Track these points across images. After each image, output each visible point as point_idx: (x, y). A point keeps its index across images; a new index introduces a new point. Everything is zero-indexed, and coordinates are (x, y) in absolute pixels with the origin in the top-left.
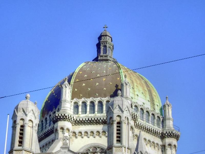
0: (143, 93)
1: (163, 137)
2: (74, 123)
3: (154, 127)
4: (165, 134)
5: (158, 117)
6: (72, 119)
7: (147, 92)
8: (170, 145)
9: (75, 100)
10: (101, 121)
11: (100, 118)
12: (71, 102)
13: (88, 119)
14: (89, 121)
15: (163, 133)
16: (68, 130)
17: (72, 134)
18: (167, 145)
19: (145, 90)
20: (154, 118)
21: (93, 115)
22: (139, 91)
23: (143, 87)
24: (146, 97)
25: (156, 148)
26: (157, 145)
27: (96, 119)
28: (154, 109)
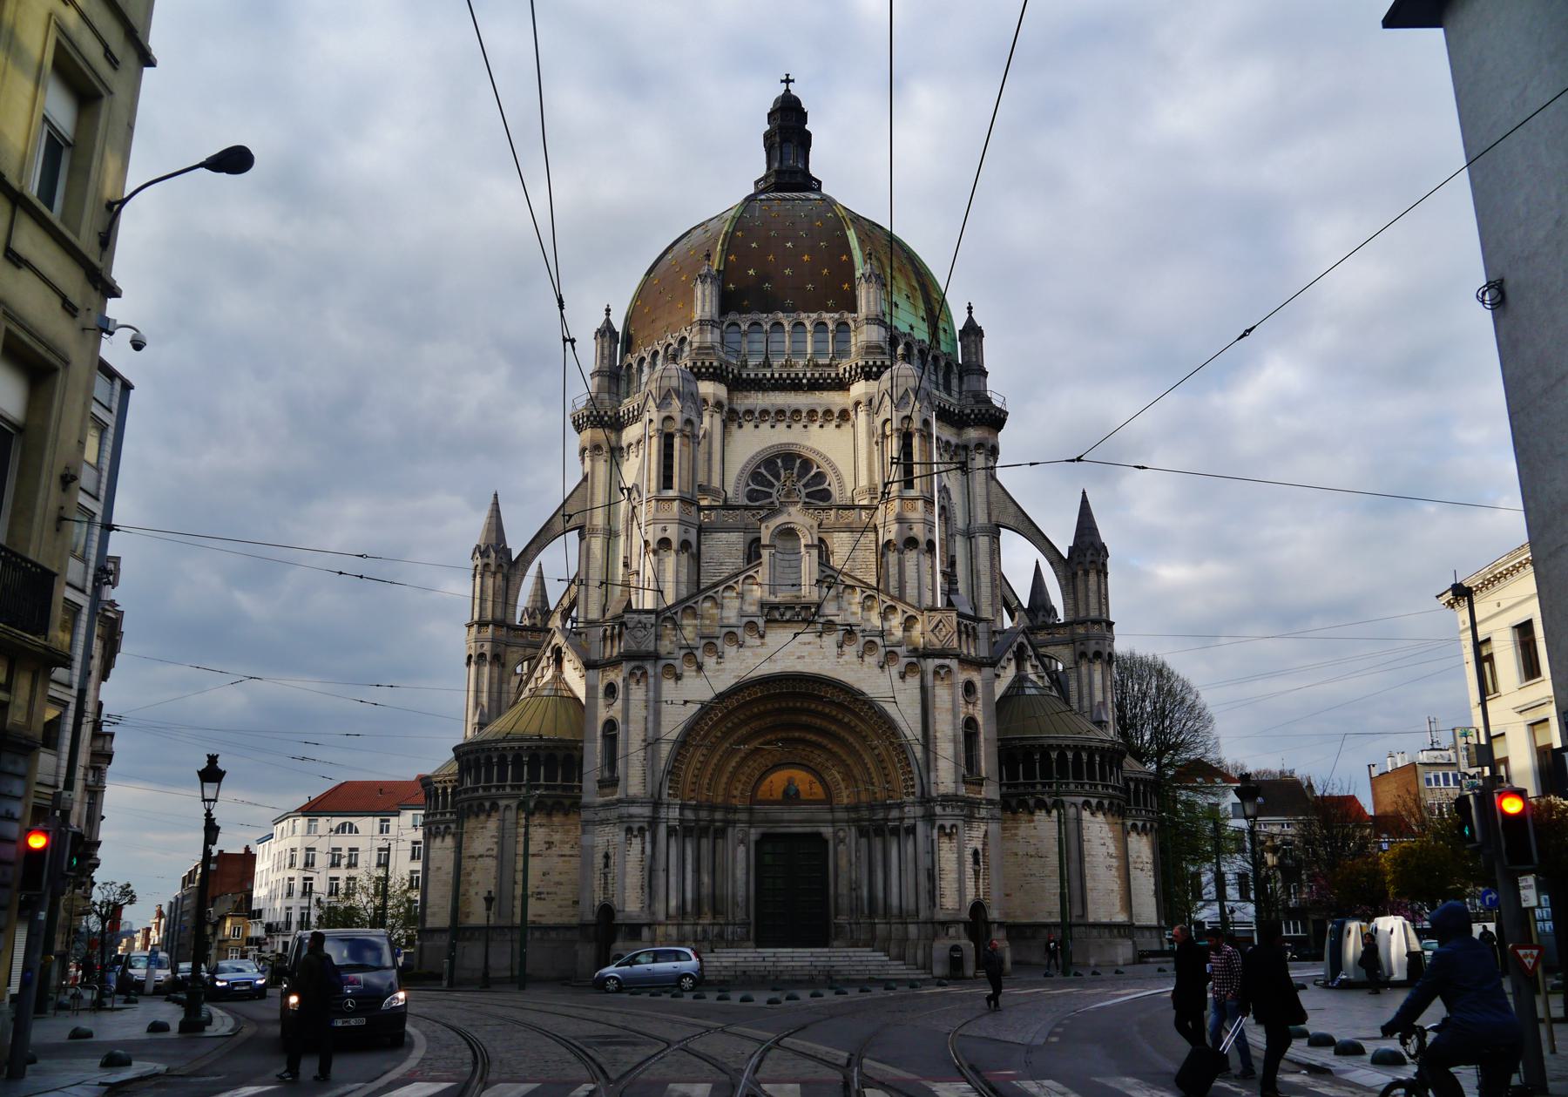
0: (908, 297)
4: (968, 415)
6: (731, 376)
7: (919, 294)
9: (732, 317)
10: (805, 381)
11: (805, 374)
12: (723, 322)
13: (772, 375)
14: (773, 381)
19: (916, 290)
22: (900, 290)
23: (907, 277)
24: (915, 307)
27: (793, 376)
28: (938, 342)
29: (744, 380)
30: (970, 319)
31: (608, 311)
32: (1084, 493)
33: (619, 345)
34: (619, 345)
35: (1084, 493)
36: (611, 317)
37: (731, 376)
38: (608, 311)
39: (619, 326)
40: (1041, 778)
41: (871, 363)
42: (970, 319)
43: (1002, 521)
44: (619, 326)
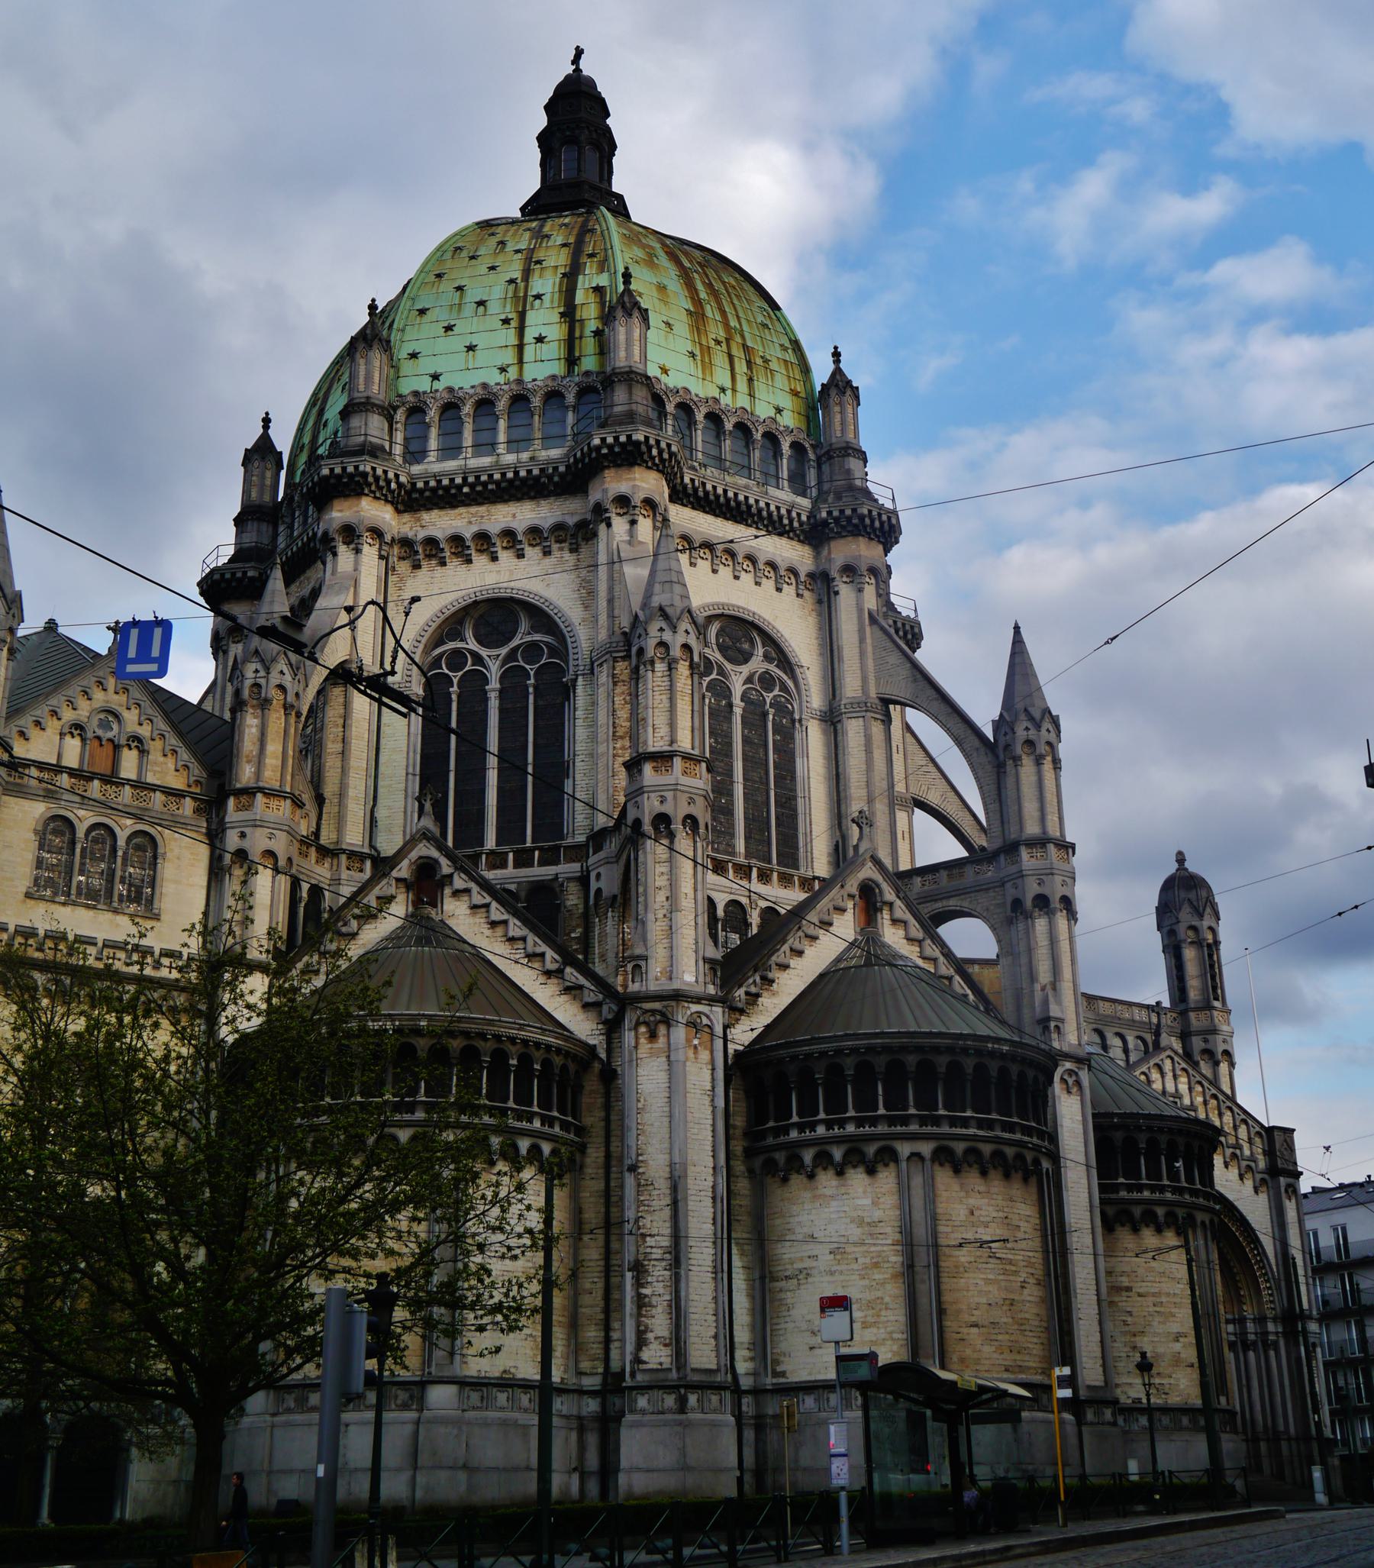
1: (815, 534)
2: (403, 502)
3: (772, 491)
5: (796, 446)
6: (393, 486)
8: (849, 570)
15: (815, 516)
16: (377, 533)
17: (396, 550)
18: (834, 574)
20: (777, 453)
21: (486, 461)
25: (789, 590)
26: (792, 577)
29: (421, 491)
30: (838, 372)
31: (267, 421)
32: (1017, 628)
33: (283, 474)
34: (283, 474)
35: (1017, 628)
36: (270, 431)
37: (393, 486)
38: (267, 421)
39: (283, 441)
40: (857, 1109)
41: (610, 440)
42: (838, 372)
43: (893, 691)
44: (283, 441)
